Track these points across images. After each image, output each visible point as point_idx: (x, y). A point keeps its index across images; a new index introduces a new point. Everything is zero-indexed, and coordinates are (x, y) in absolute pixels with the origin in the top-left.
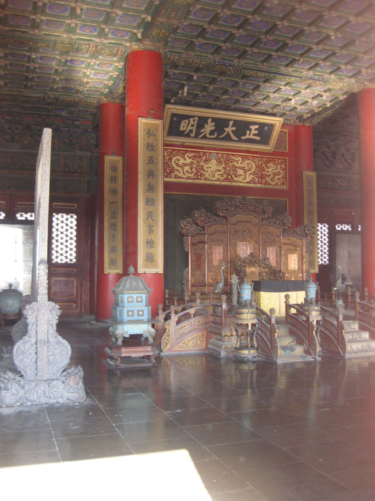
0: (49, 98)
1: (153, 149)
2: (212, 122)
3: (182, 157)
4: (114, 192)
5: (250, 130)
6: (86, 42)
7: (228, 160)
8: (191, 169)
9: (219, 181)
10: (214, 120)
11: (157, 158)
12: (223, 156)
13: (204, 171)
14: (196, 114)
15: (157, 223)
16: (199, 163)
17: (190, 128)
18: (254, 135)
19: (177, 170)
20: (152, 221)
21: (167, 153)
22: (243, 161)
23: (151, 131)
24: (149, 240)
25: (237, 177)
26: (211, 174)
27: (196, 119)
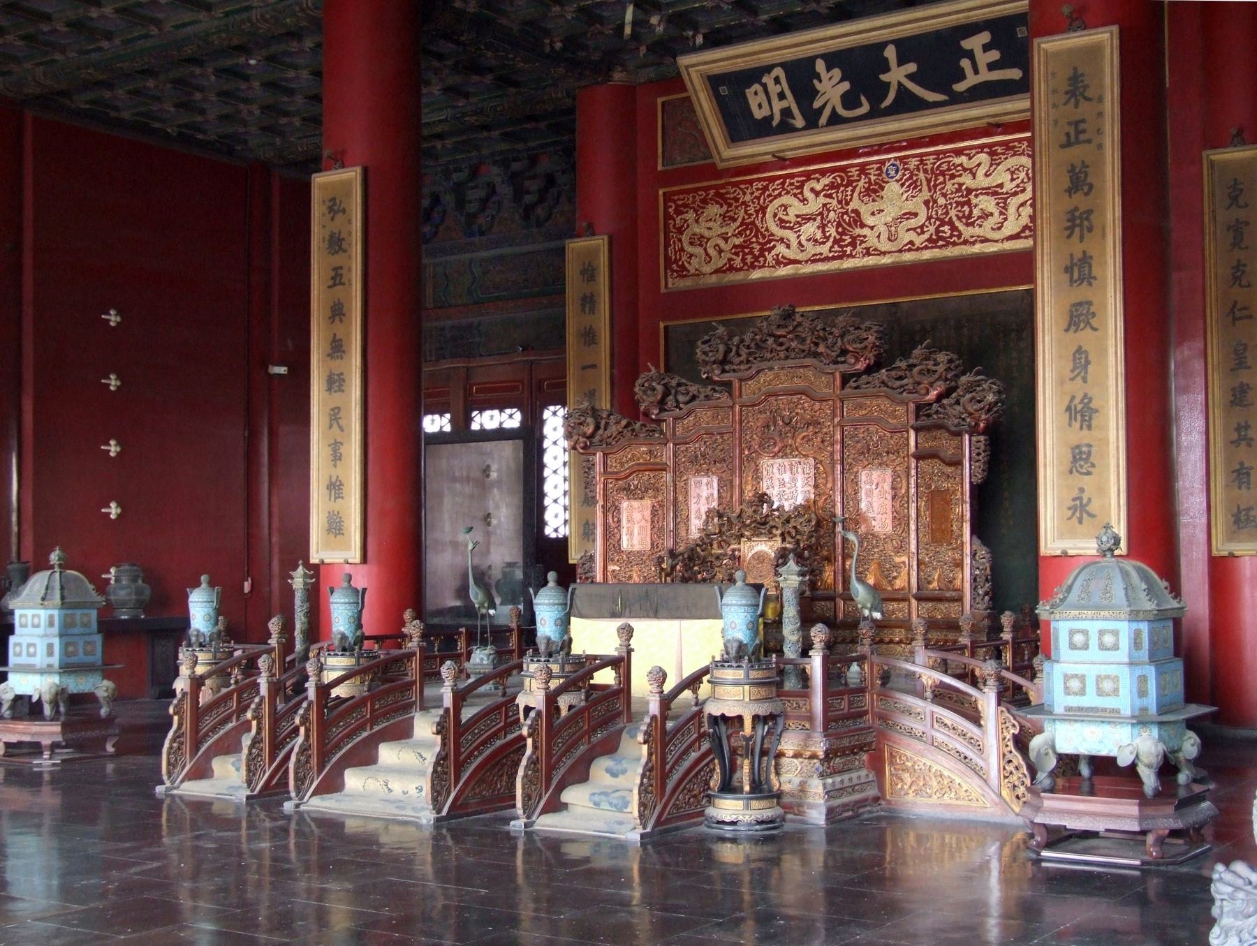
0: (464, 115)
1: (341, 248)
2: (829, 69)
3: (795, 195)
4: (589, 336)
5: (970, 55)
6: (245, 15)
7: (943, 174)
8: (823, 227)
9: (910, 250)
10: (832, 59)
11: (350, 270)
12: (921, 161)
13: (863, 226)
14: (767, 58)
15: (350, 434)
16: (847, 203)
17: (778, 106)
18: (992, 66)
19: (782, 240)
20: (338, 431)
21: (752, 193)
22: (994, 163)
23: (338, 201)
24: (334, 480)
25: (972, 224)
26: (884, 237)
27: (779, 72)
